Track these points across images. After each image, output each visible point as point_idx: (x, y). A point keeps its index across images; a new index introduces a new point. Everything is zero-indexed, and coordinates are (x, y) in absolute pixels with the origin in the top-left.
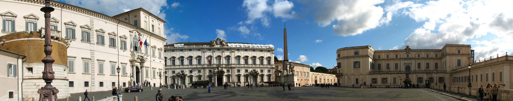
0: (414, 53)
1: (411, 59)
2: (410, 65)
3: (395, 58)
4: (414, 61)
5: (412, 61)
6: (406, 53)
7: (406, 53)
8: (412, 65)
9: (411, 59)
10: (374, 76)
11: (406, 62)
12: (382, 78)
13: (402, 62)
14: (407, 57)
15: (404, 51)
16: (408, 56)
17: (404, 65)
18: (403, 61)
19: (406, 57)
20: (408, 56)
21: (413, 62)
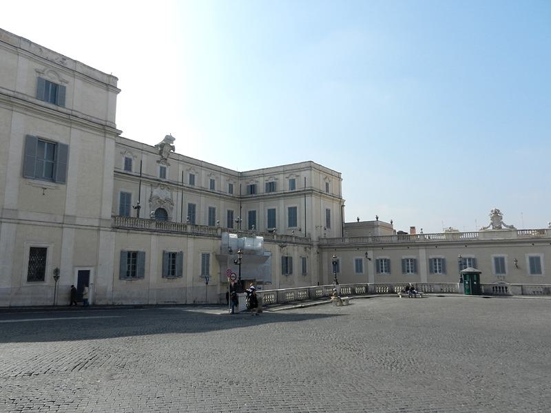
0: (181, 168)
1: (170, 185)
2: (167, 206)
3: (123, 171)
4: (180, 194)
5: (175, 194)
6: (158, 162)
7: (158, 162)
8: (175, 207)
9: (170, 185)
10: (134, 242)
11: (156, 192)
12: (164, 252)
13: (146, 190)
14: (161, 177)
15: (153, 151)
16: (163, 171)
17: (150, 206)
18: (149, 189)
19: (158, 177)
20: (163, 171)
21: (176, 196)
